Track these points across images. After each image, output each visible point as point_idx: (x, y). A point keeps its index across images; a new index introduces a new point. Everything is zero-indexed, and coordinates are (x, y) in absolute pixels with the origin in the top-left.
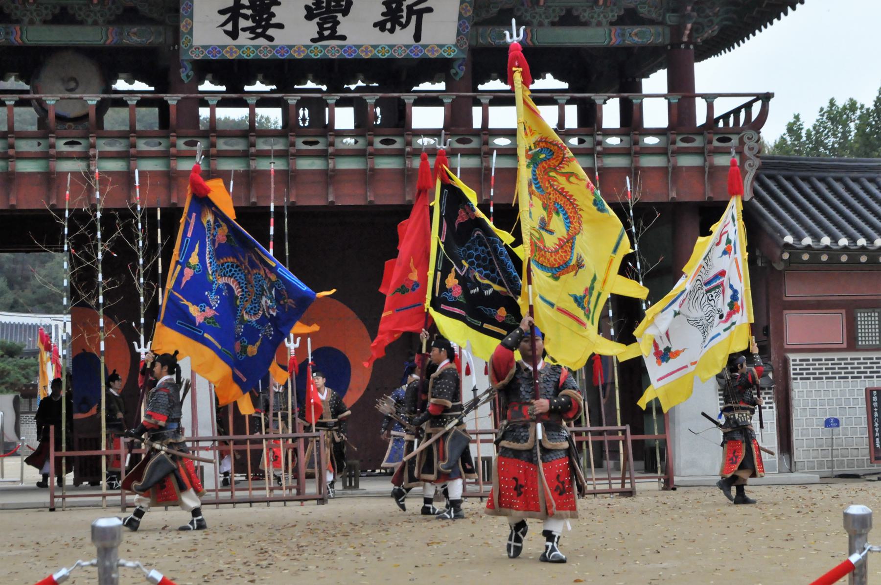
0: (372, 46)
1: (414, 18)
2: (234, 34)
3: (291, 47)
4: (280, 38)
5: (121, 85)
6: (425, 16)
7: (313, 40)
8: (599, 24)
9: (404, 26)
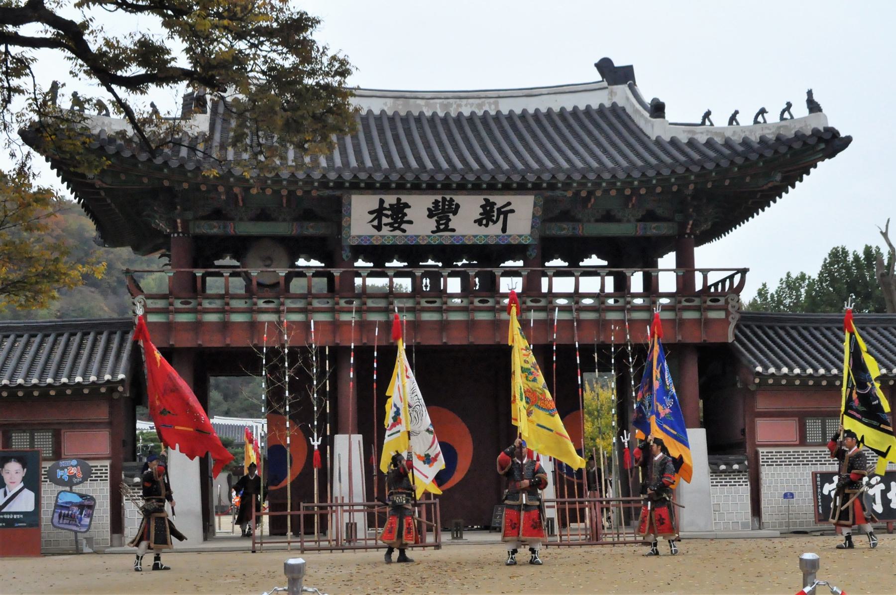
1: (502, 217)
2: (378, 228)
3: (418, 236)
5: (301, 262)
7: (433, 232)
8: (629, 221)
9: (495, 222)
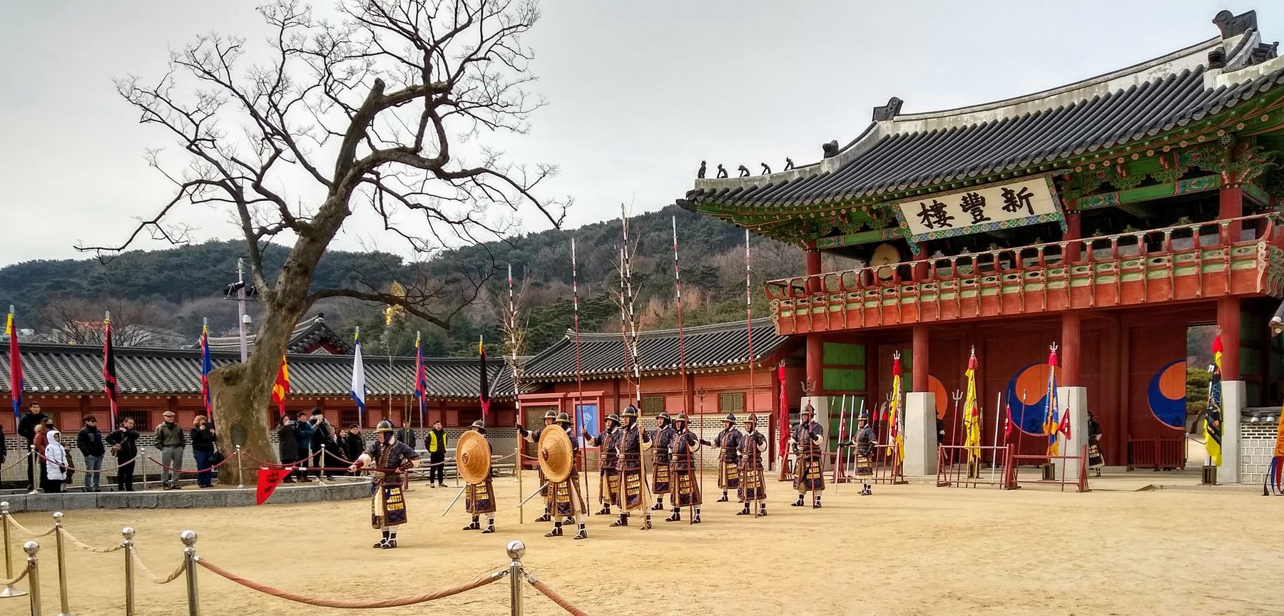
2: (930, 226)
4: (956, 224)
8: (1168, 181)
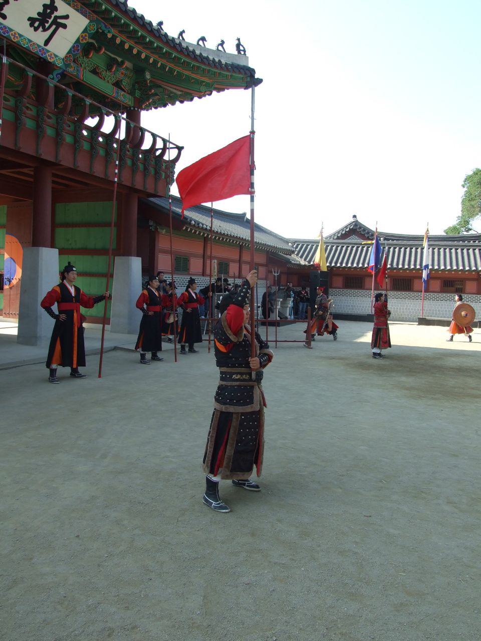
0: (19, 34)
1: (54, 27)
6: (61, 29)
